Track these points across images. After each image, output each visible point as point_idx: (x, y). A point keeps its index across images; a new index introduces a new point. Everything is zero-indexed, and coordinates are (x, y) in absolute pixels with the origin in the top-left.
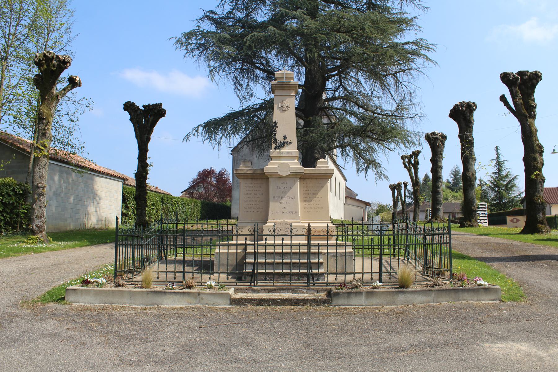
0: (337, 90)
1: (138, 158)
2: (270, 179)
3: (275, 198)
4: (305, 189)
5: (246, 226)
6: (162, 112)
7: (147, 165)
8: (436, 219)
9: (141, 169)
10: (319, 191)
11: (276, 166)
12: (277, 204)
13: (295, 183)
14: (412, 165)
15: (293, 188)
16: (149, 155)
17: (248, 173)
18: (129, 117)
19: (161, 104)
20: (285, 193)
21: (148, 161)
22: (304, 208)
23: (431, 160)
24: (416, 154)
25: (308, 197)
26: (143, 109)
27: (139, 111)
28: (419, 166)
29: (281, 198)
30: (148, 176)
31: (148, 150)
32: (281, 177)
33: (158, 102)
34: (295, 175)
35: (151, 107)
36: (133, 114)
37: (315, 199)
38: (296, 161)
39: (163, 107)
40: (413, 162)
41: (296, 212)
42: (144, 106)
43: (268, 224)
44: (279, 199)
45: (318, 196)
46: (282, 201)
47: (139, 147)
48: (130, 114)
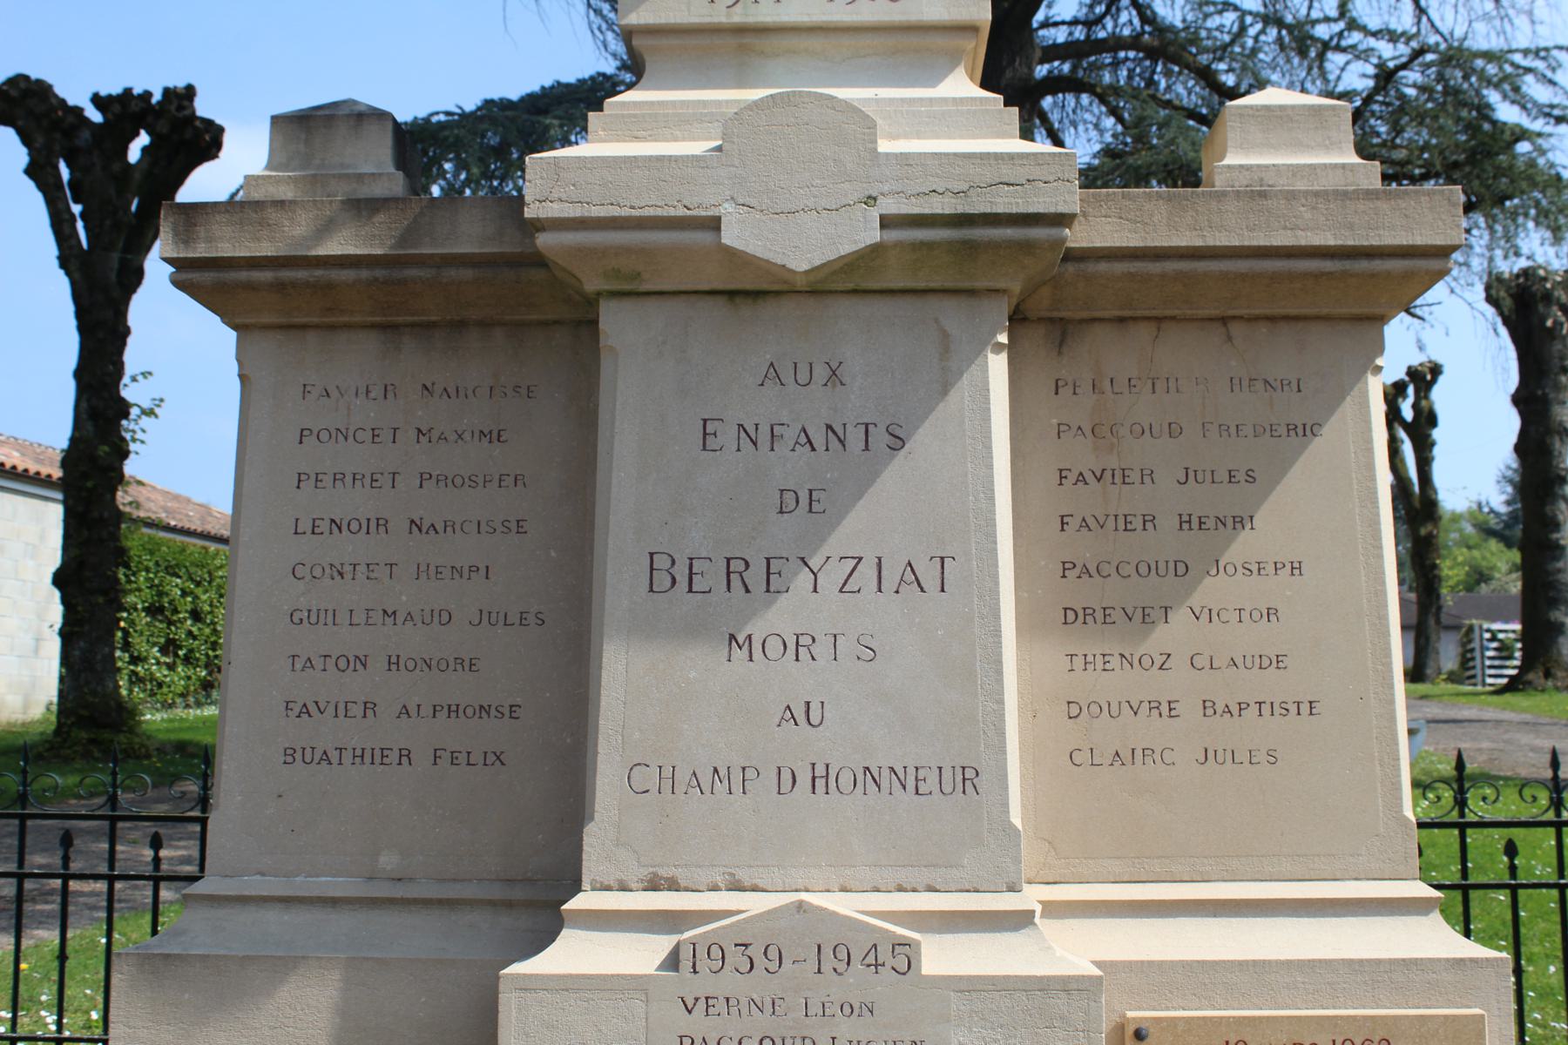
0: (1099, 20)
1: (79, 374)
2: (615, 322)
3: (669, 575)
4: (1083, 456)
5: (281, 965)
6: (198, 134)
7: (123, 409)
8: (1548, 674)
9: (89, 427)
10: (1254, 481)
11: (697, 148)
12: (701, 667)
13: (948, 366)
14: (1408, 428)
15: (923, 440)
16: (133, 357)
17: (333, 247)
18: (21, 156)
19: (190, 92)
20: (814, 506)
21: (129, 392)
22: (1074, 710)
23: (1518, 400)
24: (1424, 378)
25: (1122, 564)
26: (95, 116)
27: (86, 135)
28: (1436, 434)
30: (130, 468)
31: (127, 331)
32: (752, 291)
33: (180, 83)
34: (955, 263)
35: (135, 107)
36: (40, 141)
37: (1211, 590)
38: (961, 85)
39: (203, 108)
40: (1408, 413)
41: (968, 779)
42: (97, 100)
43: (570, 954)
44: (724, 586)
45: (1243, 547)
46: (776, 619)
47: (79, 315)
48: (26, 140)
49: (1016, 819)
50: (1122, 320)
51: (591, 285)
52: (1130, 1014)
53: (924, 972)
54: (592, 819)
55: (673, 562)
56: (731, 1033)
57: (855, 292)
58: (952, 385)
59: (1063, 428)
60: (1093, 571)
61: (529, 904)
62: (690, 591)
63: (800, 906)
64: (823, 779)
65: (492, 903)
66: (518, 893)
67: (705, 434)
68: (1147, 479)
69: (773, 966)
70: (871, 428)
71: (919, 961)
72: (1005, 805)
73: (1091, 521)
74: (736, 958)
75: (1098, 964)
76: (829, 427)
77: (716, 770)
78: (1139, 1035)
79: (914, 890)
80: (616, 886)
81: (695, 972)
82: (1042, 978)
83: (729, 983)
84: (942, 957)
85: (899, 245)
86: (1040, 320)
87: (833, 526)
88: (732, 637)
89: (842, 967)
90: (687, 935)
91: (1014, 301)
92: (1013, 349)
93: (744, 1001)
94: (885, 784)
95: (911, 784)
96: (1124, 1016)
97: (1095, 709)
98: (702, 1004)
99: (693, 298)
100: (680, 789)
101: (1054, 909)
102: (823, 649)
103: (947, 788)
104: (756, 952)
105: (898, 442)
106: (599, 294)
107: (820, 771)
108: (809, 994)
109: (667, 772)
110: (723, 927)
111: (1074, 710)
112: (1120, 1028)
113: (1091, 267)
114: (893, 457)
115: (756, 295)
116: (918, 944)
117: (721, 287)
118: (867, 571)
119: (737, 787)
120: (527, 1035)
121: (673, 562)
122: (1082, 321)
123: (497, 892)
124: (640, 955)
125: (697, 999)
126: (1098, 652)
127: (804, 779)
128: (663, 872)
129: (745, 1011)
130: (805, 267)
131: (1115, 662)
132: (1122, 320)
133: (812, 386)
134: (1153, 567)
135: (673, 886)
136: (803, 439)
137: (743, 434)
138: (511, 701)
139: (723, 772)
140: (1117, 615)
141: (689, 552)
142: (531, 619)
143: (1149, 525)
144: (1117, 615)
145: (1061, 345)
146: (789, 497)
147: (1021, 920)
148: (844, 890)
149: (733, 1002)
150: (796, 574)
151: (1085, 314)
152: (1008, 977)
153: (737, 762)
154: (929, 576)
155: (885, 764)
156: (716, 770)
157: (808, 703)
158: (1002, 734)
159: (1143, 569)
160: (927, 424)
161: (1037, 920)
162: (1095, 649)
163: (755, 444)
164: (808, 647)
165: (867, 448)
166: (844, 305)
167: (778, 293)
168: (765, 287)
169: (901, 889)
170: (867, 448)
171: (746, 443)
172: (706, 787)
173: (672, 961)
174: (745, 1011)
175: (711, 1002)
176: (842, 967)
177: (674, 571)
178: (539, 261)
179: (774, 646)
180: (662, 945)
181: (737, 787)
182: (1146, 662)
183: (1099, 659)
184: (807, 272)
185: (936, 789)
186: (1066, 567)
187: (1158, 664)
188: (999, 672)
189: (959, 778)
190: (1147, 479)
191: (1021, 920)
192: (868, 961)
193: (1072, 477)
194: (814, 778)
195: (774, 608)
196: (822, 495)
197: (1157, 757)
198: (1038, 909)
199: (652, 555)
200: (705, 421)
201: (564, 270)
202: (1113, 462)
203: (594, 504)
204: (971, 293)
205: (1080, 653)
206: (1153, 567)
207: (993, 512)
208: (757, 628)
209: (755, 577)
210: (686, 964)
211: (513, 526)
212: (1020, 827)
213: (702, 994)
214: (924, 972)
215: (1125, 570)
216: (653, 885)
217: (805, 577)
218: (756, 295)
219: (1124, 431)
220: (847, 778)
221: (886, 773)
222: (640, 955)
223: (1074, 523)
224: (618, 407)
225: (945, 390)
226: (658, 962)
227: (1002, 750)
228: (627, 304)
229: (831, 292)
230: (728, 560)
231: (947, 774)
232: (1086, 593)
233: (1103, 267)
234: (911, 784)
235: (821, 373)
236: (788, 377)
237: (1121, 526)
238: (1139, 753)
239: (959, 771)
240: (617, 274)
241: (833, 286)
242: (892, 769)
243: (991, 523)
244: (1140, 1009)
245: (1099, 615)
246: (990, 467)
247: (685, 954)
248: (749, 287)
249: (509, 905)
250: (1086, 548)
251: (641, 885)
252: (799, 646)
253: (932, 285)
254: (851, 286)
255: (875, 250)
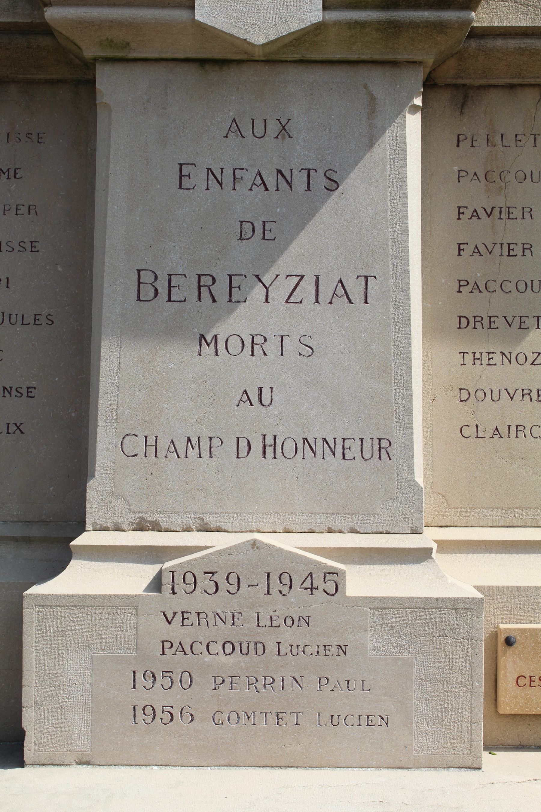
3: (152, 287)
4: (477, 196)
12: (179, 360)
13: (374, 125)
15: (354, 183)
20: (267, 234)
22: (464, 395)
29: (220, 290)
41: (383, 448)
43: (77, 579)
44: (195, 298)
46: (238, 323)
49: (419, 479)
50: (512, 87)
51: (89, 52)
52: (502, 626)
53: (348, 594)
54: (93, 476)
55: (156, 278)
56: (201, 639)
57: (301, 62)
58: (377, 139)
59: (462, 174)
60: (482, 288)
61: (44, 540)
62: (169, 300)
63: (254, 544)
64: (270, 447)
65: (15, 539)
66: (35, 532)
67: (181, 176)
68: (527, 216)
69: (233, 589)
70: (312, 172)
71: (344, 586)
72: (411, 468)
73: (482, 249)
74: (204, 582)
75: (479, 588)
76: (279, 172)
77: (189, 439)
78: (509, 642)
79: (341, 532)
80: (112, 527)
81: (174, 593)
82: (437, 599)
83: (199, 601)
84: (362, 583)
85: (338, 23)
86: (447, 86)
87: (282, 251)
88: (202, 337)
89: (285, 590)
90: (168, 565)
91: (428, 70)
92: (426, 112)
93: (211, 615)
94: (319, 451)
95: (339, 451)
96: (498, 627)
97: (480, 394)
98: (179, 617)
99: (171, 65)
100: (161, 453)
101: (446, 546)
102: (272, 347)
103: (367, 455)
104: (220, 578)
105: (333, 185)
106: (96, 59)
107: (269, 440)
108: (261, 610)
109: (151, 441)
110: (196, 560)
111: (465, 395)
112: (494, 636)
113: (490, 43)
114: (329, 196)
115: (222, 63)
116: (344, 573)
117: (193, 55)
118: (308, 286)
119: (205, 453)
120: (45, 640)
121: (156, 278)
122: (480, 87)
123: (18, 531)
124: (132, 580)
125: (175, 613)
126: (484, 351)
127: (257, 447)
128: (147, 517)
129: (212, 622)
130: (260, 41)
131: (497, 358)
132: (512, 87)
133: (266, 138)
134: (529, 285)
135: (156, 527)
136: (259, 181)
137: (211, 176)
138: (28, 384)
139: (194, 441)
140: (500, 322)
141: (168, 270)
142: (43, 320)
143: (527, 252)
144: (500, 322)
145: (462, 107)
146: (247, 227)
147: (422, 555)
148: (287, 531)
149: (202, 616)
150: (252, 288)
151: (483, 82)
152: (412, 598)
153: (206, 434)
154: (355, 289)
155: (320, 436)
156: (189, 439)
157: (260, 389)
158: (410, 413)
159: (522, 287)
160: (356, 170)
161: (434, 555)
162: (482, 348)
163: (220, 184)
164: (261, 345)
165: (309, 189)
166: (293, 73)
167: (240, 62)
168: (230, 56)
169: (330, 531)
170: (309, 189)
171: (213, 182)
172: (182, 453)
173: (156, 585)
174: (212, 622)
175: (186, 615)
176: (285, 590)
177: (157, 284)
178: (46, 30)
179: (235, 343)
180: (149, 571)
181: (205, 453)
182: (521, 358)
183: (485, 355)
184: (263, 45)
185: (358, 455)
186: (461, 284)
187: (530, 360)
188: (409, 366)
189: (376, 447)
190: (527, 216)
191: (422, 555)
192: (305, 585)
193: (468, 213)
194: (264, 446)
195: (235, 315)
196: (273, 226)
197: (527, 432)
198: (435, 546)
199: (139, 271)
200: (181, 165)
201: (67, 39)
202: (500, 202)
203: (92, 230)
204: (394, 64)
205: (470, 351)
206: (529, 285)
207: (407, 241)
208: (222, 330)
209: (221, 289)
210: (167, 588)
211: (28, 246)
212: (423, 487)
213: (179, 609)
214: (348, 594)
215: (508, 287)
216: (141, 527)
217: (259, 291)
218: (222, 63)
219: (510, 177)
220: (289, 447)
221: (320, 442)
222: (132, 580)
223: (468, 249)
224: (112, 152)
225: (371, 144)
226: (145, 585)
227: (410, 427)
228: (119, 68)
229: (282, 62)
230: (199, 276)
231: (367, 444)
232: (477, 305)
233: (499, 43)
234: (339, 451)
235: (273, 128)
236: (247, 130)
237: (505, 252)
238: (513, 429)
239: (376, 442)
240: (110, 43)
241: (283, 57)
242: (325, 440)
243: (405, 249)
244: (510, 622)
245: (486, 322)
246: (406, 205)
247: (167, 579)
248: (217, 56)
249: (28, 540)
250: (477, 269)
251: (131, 527)
252: (254, 344)
253: (363, 57)
254: (297, 57)
255: (318, 28)
